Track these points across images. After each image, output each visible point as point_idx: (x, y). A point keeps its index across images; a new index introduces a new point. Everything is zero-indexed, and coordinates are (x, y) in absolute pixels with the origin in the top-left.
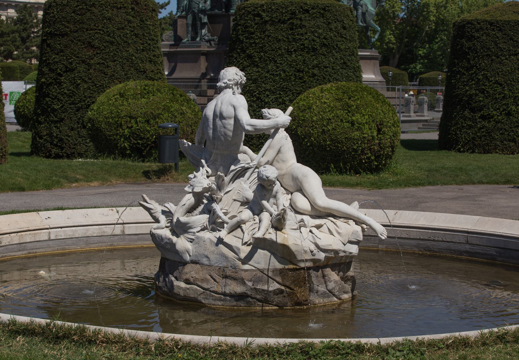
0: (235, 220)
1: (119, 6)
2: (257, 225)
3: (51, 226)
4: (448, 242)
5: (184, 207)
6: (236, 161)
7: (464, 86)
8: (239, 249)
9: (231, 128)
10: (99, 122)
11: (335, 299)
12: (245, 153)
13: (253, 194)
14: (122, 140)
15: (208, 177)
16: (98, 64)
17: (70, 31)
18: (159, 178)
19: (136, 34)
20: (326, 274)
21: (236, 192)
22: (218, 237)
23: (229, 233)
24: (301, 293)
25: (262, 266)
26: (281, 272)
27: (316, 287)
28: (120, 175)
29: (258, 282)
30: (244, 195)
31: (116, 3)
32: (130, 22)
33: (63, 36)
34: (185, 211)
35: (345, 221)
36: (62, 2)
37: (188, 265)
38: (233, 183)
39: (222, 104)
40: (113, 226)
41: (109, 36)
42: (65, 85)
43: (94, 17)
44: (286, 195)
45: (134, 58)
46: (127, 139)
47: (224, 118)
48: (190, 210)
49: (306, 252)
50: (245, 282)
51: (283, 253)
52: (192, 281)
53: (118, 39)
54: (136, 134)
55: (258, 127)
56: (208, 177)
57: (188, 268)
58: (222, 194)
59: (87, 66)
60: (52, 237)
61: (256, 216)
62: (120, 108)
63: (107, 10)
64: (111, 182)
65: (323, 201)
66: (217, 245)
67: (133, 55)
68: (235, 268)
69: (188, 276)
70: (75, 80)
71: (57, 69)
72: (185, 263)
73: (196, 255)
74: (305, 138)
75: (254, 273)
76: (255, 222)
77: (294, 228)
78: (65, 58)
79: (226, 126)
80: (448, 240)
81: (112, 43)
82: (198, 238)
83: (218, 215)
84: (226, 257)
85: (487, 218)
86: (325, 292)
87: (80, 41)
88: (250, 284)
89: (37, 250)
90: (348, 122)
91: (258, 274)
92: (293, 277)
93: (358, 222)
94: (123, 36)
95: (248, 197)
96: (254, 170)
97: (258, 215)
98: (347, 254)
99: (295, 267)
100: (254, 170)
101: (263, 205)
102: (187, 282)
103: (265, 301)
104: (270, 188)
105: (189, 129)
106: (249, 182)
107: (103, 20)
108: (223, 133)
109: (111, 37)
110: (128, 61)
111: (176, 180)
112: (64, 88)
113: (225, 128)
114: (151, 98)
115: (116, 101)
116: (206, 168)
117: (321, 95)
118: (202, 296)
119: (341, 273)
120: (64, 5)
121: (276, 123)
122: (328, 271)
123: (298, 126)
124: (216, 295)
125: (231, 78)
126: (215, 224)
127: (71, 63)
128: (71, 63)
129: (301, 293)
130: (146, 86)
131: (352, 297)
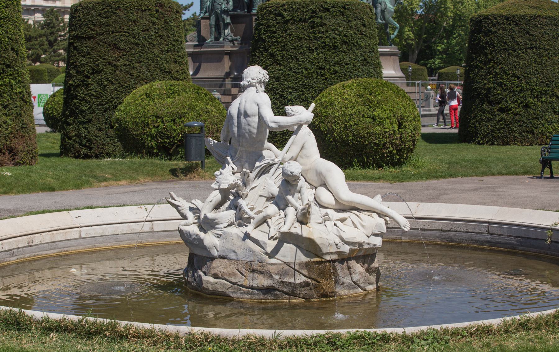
0: (261, 216)
1: (143, 9)
2: (283, 220)
3: (82, 225)
4: (469, 232)
6: (260, 157)
7: (482, 79)
8: (265, 243)
9: (255, 125)
10: (126, 122)
11: (361, 290)
13: (278, 190)
14: (149, 139)
15: (234, 173)
16: (125, 65)
17: (97, 34)
18: (186, 176)
19: (160, 36)
20: (351, 266)
21: (262, 188)
24: (326, 285)
25: (288, 260)
26: (307, 265)
27: (341, 279)
28: (148, 173)
29: (284, 276)
31: (140, 6)
32: (154, 23)
33: (89, 38)
34: (212, 208)
35: (369, 214)
36: (88, 6)
37: (216, 260)
38: (258, 179)
39: (246, 102)
40: (143, 223)
41: (134, 37)
42: (93, 86)
43: (119, 20)
45: (159, 59)
46: (153, 138)
47: (248, 116)
48: (217, 207)
49: (330, 245)
50: (272, 276)
51: (309, 246)
52: (220, 275)
53: (143, 41)
54: (162, 133)
55: (282, 124)
56: (234, 173)
57: (216, 263)
58: (248, 190)
59: (113, 68)
60: (83, 236)
61: (281, 211)
62: (146, 108)
63: (131, 13)
64: (139, 180)
65: (347, 194)
66: (244, 240)
67: (158, 56)
69: (216, 271)
70: (101, 81)
71: (84, 71)
72: (213, 259)
73: (223, 251)
74: (328, 133)
75: (281, 266)
76: (281, 217)
77: (318, 221)
78: (91, 60)
79: (251, 124)
80: (470, 231)
81: (137, 45)
82: (225, 233)
83: (244, 211)
84: (253, 252)
85: (507, 209)
86: (350, 284)
87: (106, 43)
88: (277, 277)
89: (68, 249)
90: (370, 117)
91: (285, 268)
92: (319, 269)
93: (381, 215)
94: (148, 37)
95: (273, 192)
97: (283, 210)
98: (372, 246)
99: (320, 259)
102: (216, 276)
103: (292, 294)
104: (294, 183)
105: (215, 128)
107: (128, 23)
108: (247, 131)
109: (136, 39)
110: (153, 62)
111: (202, 178)
112: (91, 90)
113: (249, 125)
114: (177, 98)
115: (143, 101)
116: (232, 164)
117: (342, 91)
118: (230, 290)
119: (366, 265)
120: (90, 8)
121: (299, 119)
122: (353, 263)
123: (321, 122)
124: (244, 289)
125: (255, 76)
126: (242, 219)
127: (98, 65)
128: (98, 65)
129: (326, 285)
130: (171, 86)
131: (377, 288)
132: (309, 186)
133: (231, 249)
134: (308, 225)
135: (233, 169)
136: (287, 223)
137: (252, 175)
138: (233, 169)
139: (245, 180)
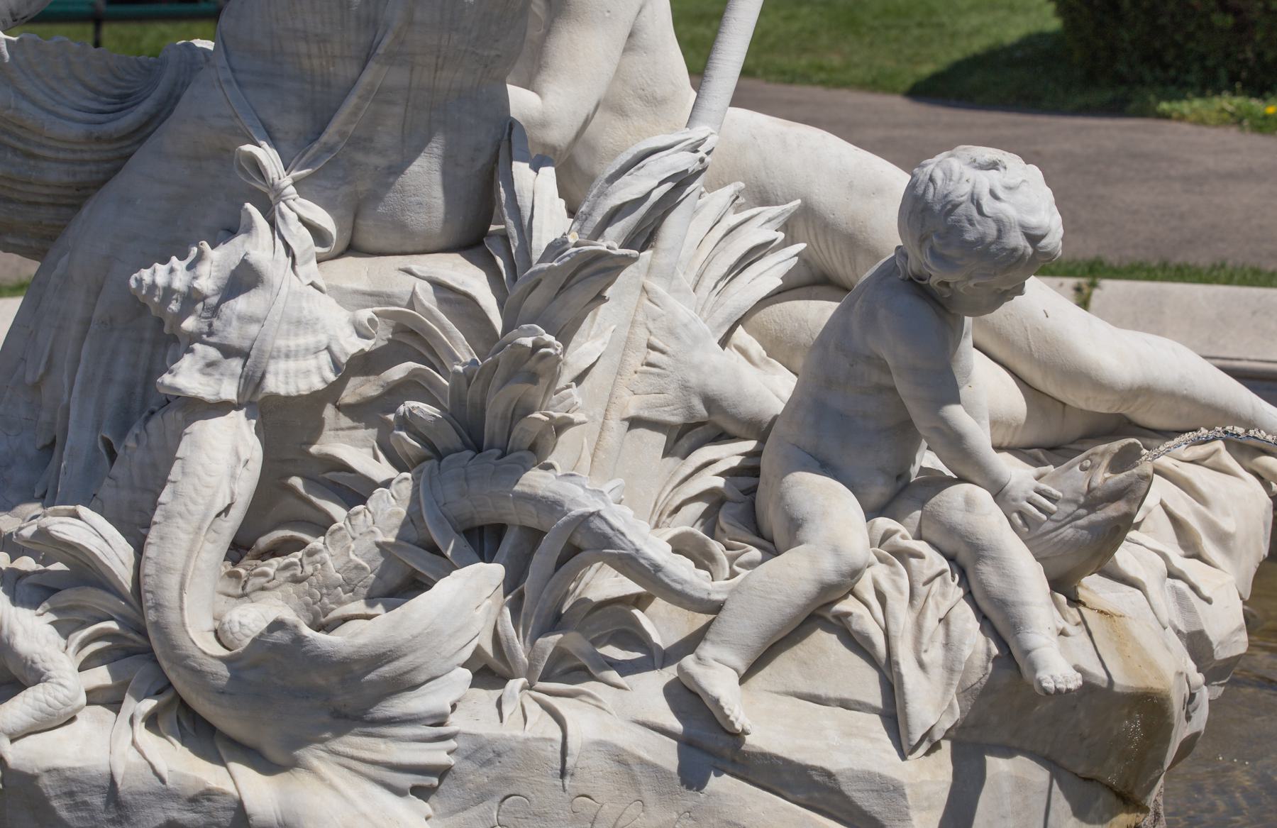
8: (891, 790)
21: (635, 361)
30: (693, 379)
66: (692, 777)
82: (484, 752)
135: (318, 234)
138: (318, 234)
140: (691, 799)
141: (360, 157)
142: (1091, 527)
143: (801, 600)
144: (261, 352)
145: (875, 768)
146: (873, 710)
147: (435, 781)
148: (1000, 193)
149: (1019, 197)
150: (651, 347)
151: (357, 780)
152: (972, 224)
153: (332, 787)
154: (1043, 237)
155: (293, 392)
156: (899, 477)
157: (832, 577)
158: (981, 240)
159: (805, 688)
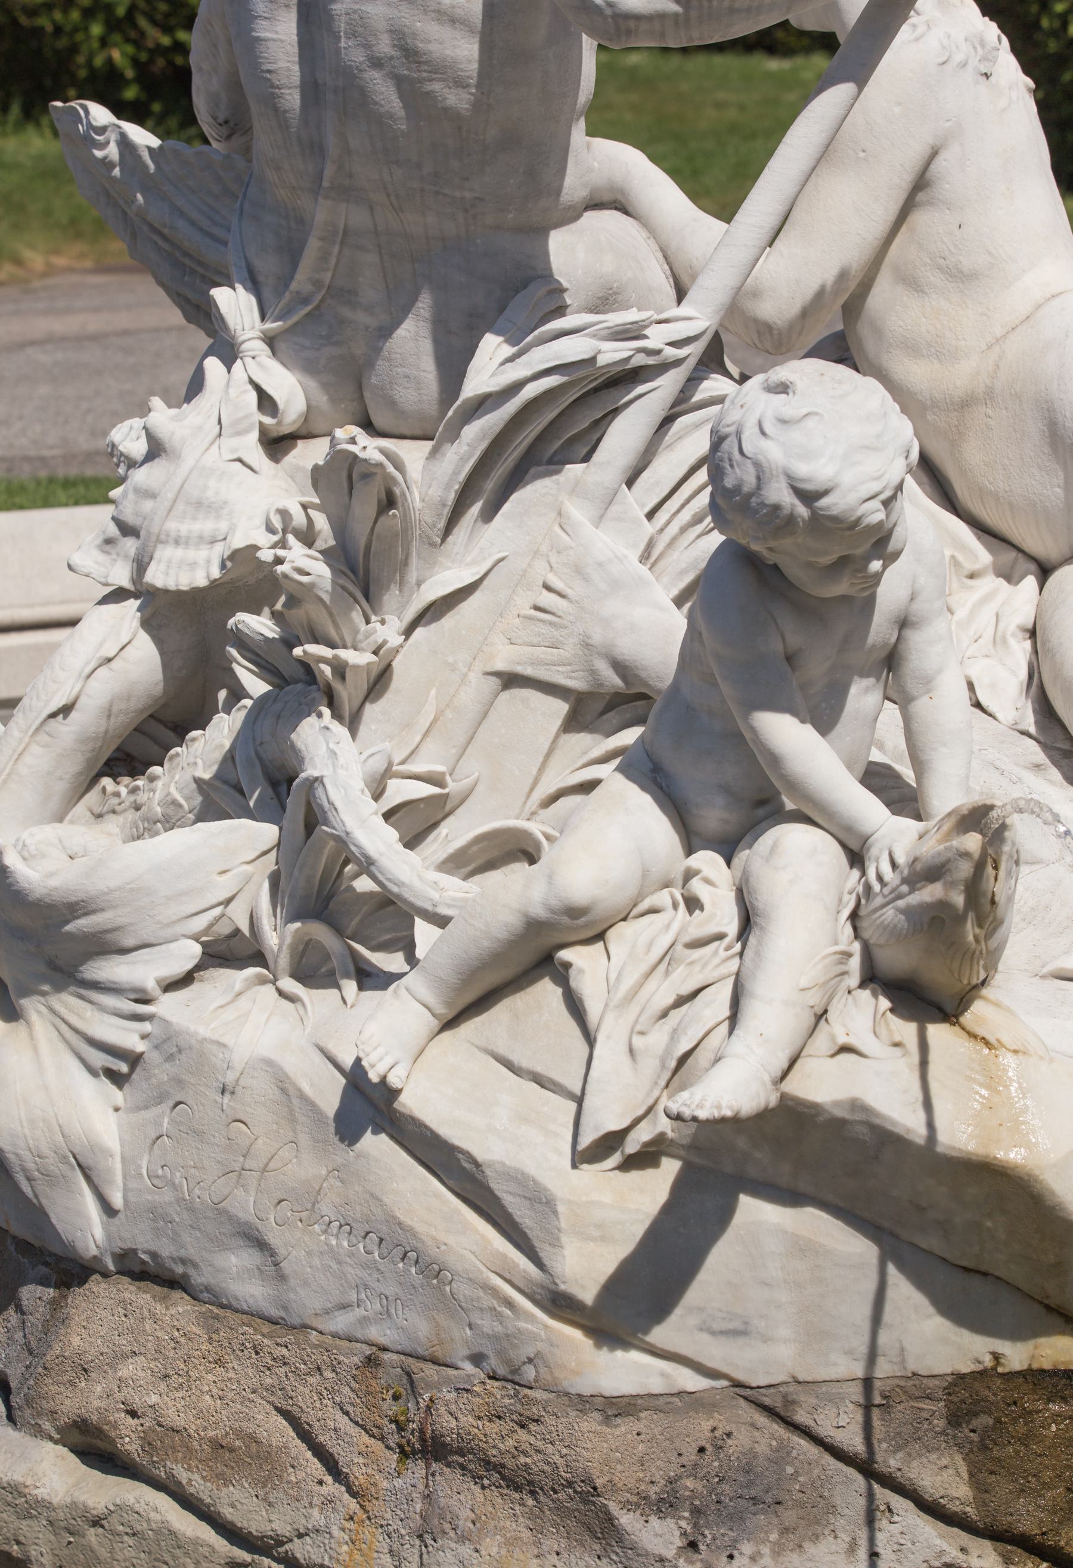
0: (506, 898)
2: (717, 964)
5: (68, 729)
6: (522, 295)
8: (543, 1201)
12: (615, 201)
13: (677, 622)
15: (276, 444)
21: (523, 604)
22: (348, 1062)
23: (450, 1024)
26: (970, 1406)
28: (73, 221)
29: (736, 1518)
30: (597, 637)
34: (73, 766)
37: (96, 1285)
38: (489, 513)
44: (992, 583)
50: (610, 1519)
56: (276, 444)
57: (99, 1316)
58: (387, 630)
61: (707, 860)
64: (18, 262)
68: (512, 1379)
69: (90, 1399)
73: (156, 1215)
75: (702, 1427)
76: (699, 925)
82: (171, 1044)
83: (342, 842)
84: (432, 1271)
91: (741, 1441)
95: (628, 647)
96: (693, 381)
97: (727, 848)
100: (693, 381)
101: (775, 760)
102: (96, 1449)
104: (841, 587)
106: (636, 501)
108: (384, 46)
126: (337, 922)
132: (981, 555)
133: (223, 1214)
134: (978, 1013)
135: (266, 402)
136: (755, 1012)
137: (426, 473)
138: (266, 402)
139: (360, 531)
140: (342, 1154)
141: (346, 312)
142: (907, 912)
143: (502, 934)
144: (149, 533)
145: (531, 1169)
146: (569, 1095)
147: (124, 1068)
148: (768, 428)
149: (795, 435)
150: (547, 588)
151: (61, 1046)
152: (732, 466)
153: (36, 1050)
154: (826, 493)
155: (172, 586)
156: (761, 803)
157: (539, 911)
158: (737, 489)
159: (502, 1050)
